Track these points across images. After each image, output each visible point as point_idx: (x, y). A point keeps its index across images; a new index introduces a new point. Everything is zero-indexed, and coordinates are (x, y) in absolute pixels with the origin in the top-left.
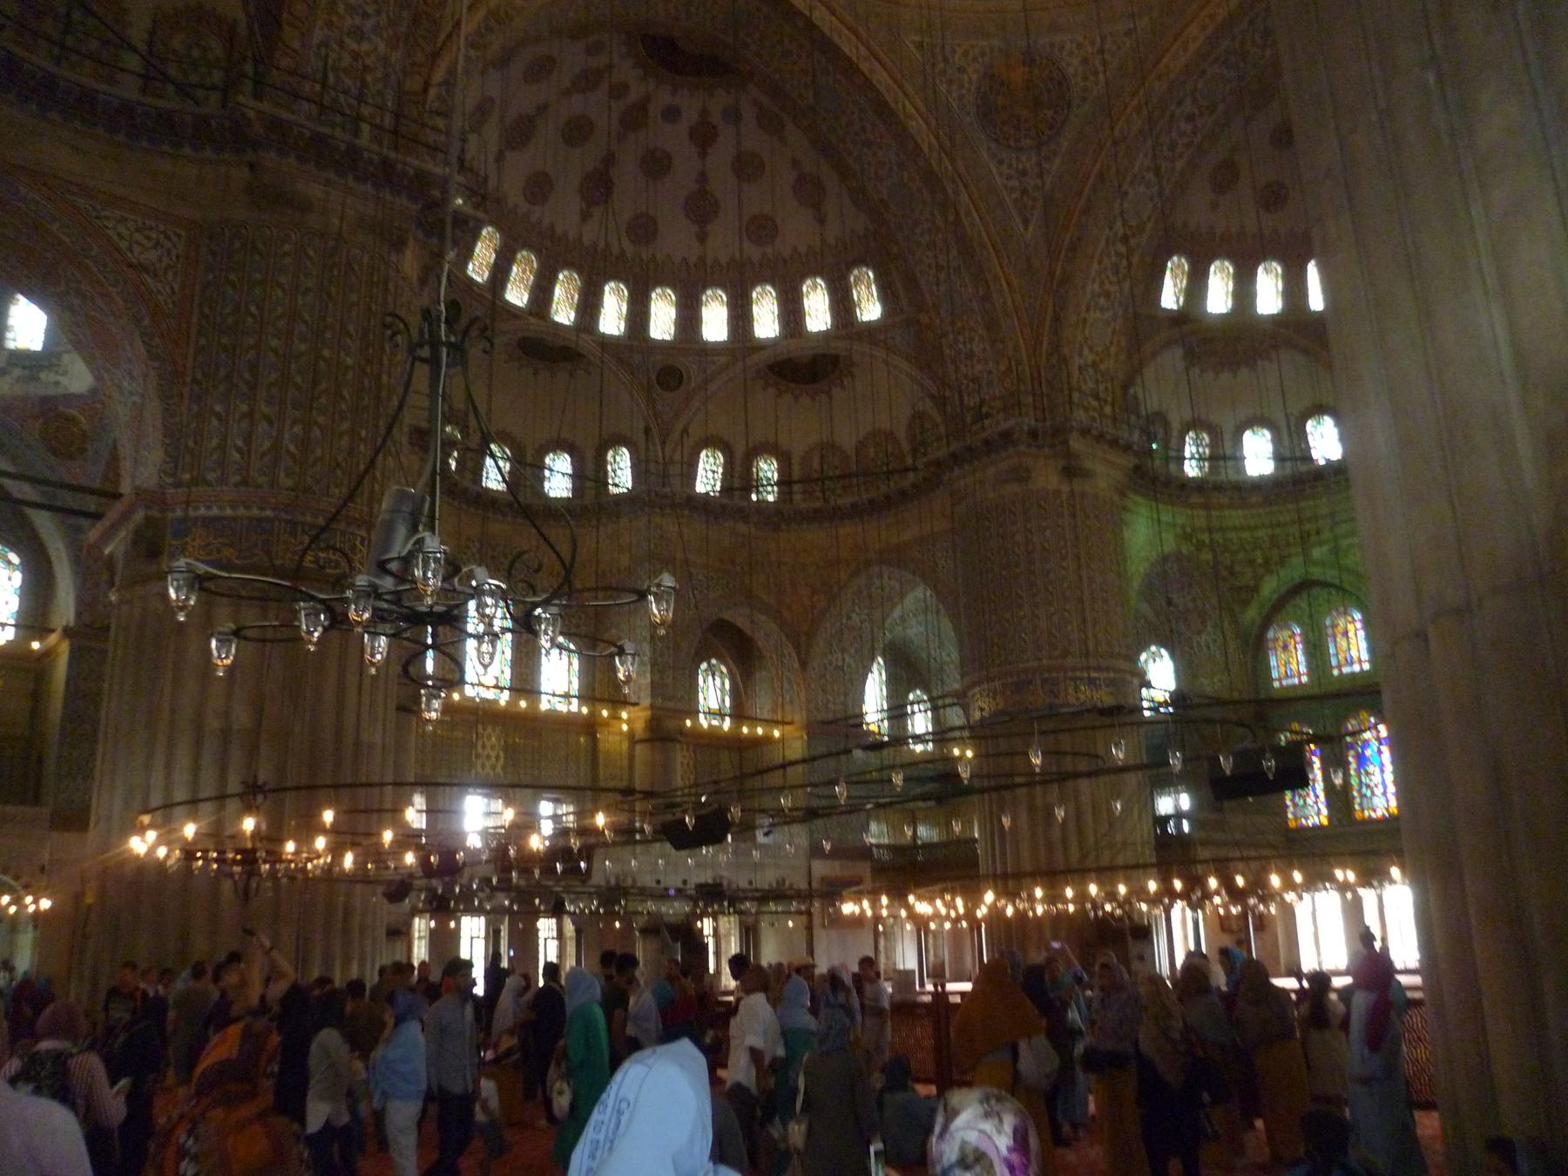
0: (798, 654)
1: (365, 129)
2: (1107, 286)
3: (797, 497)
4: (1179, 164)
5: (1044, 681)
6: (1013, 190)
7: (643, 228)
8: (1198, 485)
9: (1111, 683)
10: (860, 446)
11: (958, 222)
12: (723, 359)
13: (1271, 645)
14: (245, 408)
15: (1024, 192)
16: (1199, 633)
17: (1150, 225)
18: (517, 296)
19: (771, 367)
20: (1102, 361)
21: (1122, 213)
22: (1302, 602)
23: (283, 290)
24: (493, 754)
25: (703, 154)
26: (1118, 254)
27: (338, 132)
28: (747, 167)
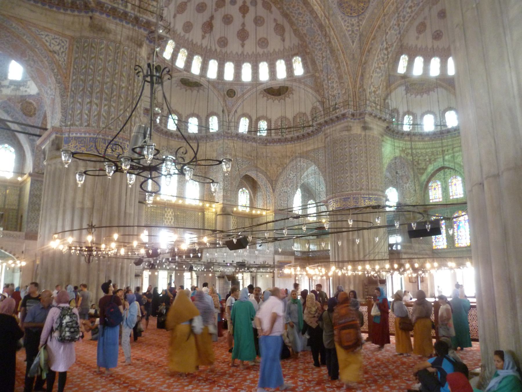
0: (272, 187)
1: (129, 5)
2: (380, 65)
3: (273, 134)
4: (406, 23)
5: (354, 198)
6: (349, 31)
7: (223, 42)
8: (409, 134)
9: (376, 199)
10: (295, 118)
11: (330, 42)
12: (249, 87)
13: (430, 188)
14: (88, 100)
15: (353, 32)
16: (406, 183)
17: (395, 44)
18: (180, 63)
19: (265, 90)
20: (377, 91)
21: (386, 39)
22: (441, 174)
23: (102, 60)
24: (170, 218)
25: (244, 17)
26: (385, 54)
27: (120, 7)
28: (258, 21)
